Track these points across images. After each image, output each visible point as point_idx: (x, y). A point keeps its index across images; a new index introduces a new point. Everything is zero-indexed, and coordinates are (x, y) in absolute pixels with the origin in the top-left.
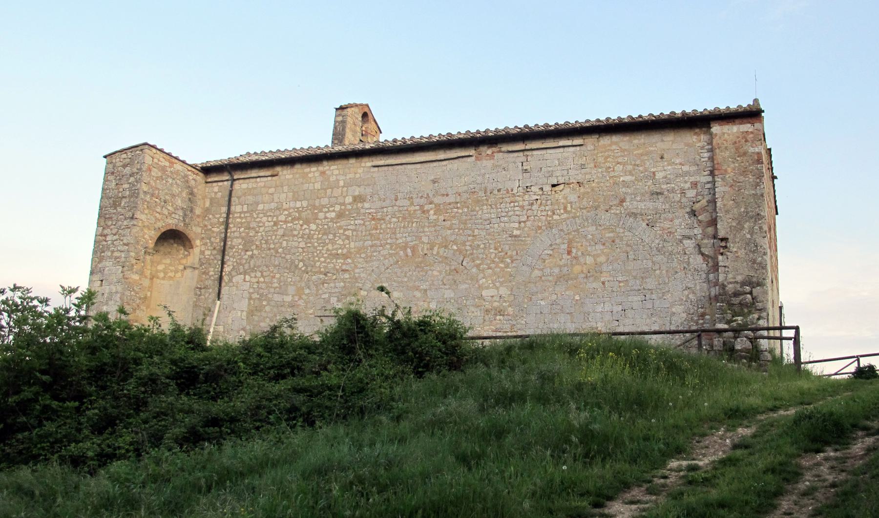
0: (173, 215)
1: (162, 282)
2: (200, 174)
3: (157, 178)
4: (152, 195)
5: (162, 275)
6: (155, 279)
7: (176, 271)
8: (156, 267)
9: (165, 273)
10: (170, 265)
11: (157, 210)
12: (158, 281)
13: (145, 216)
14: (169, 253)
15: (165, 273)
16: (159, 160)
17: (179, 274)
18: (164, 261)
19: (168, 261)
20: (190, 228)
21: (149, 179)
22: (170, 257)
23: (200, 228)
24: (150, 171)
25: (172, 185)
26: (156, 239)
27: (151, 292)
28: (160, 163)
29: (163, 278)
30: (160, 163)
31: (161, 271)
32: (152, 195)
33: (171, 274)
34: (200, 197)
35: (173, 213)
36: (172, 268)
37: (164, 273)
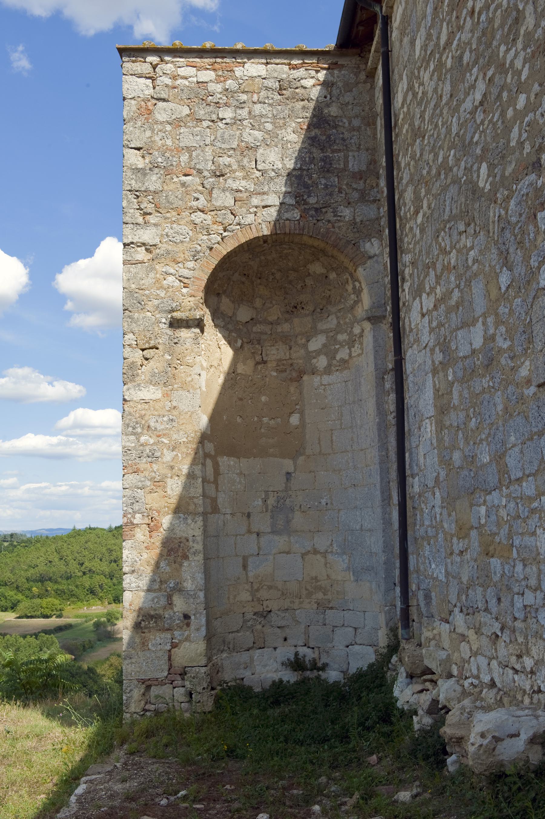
0: (255, 201)
1: (326, 379)
2: (341, 61)
3: (177, 123)
4: (168, 172)
5: (322, 362)
6: (305, 378)
7: (351, 343)
8: (305, 346)
9: (331, 355)
10: (338, 330)
11: (195, 204)
12: (316, 380)
13: (154, 230)
14: (328, 300)
15: (331, 355)
16: (174, 78)
17: (356, 350)
18: (322, 326)
19: (332, 322)
20: (330, 216)
21: (148, 133)
22: (333, 310)
23: (374, 206)
24: (150, 112)
25: (237, 121)
26: (205, 278)
27: (302, 413)
28: (179, 81)
29: (328, 370)
30: (179, 81)
31: (318, 353)
32: (168, 172)
33: (343, 354)
34: (356, 123)
35: (252, 194)
36: (342, 337)
37: (326, 354)
